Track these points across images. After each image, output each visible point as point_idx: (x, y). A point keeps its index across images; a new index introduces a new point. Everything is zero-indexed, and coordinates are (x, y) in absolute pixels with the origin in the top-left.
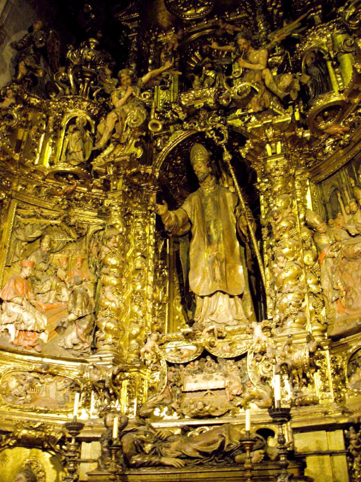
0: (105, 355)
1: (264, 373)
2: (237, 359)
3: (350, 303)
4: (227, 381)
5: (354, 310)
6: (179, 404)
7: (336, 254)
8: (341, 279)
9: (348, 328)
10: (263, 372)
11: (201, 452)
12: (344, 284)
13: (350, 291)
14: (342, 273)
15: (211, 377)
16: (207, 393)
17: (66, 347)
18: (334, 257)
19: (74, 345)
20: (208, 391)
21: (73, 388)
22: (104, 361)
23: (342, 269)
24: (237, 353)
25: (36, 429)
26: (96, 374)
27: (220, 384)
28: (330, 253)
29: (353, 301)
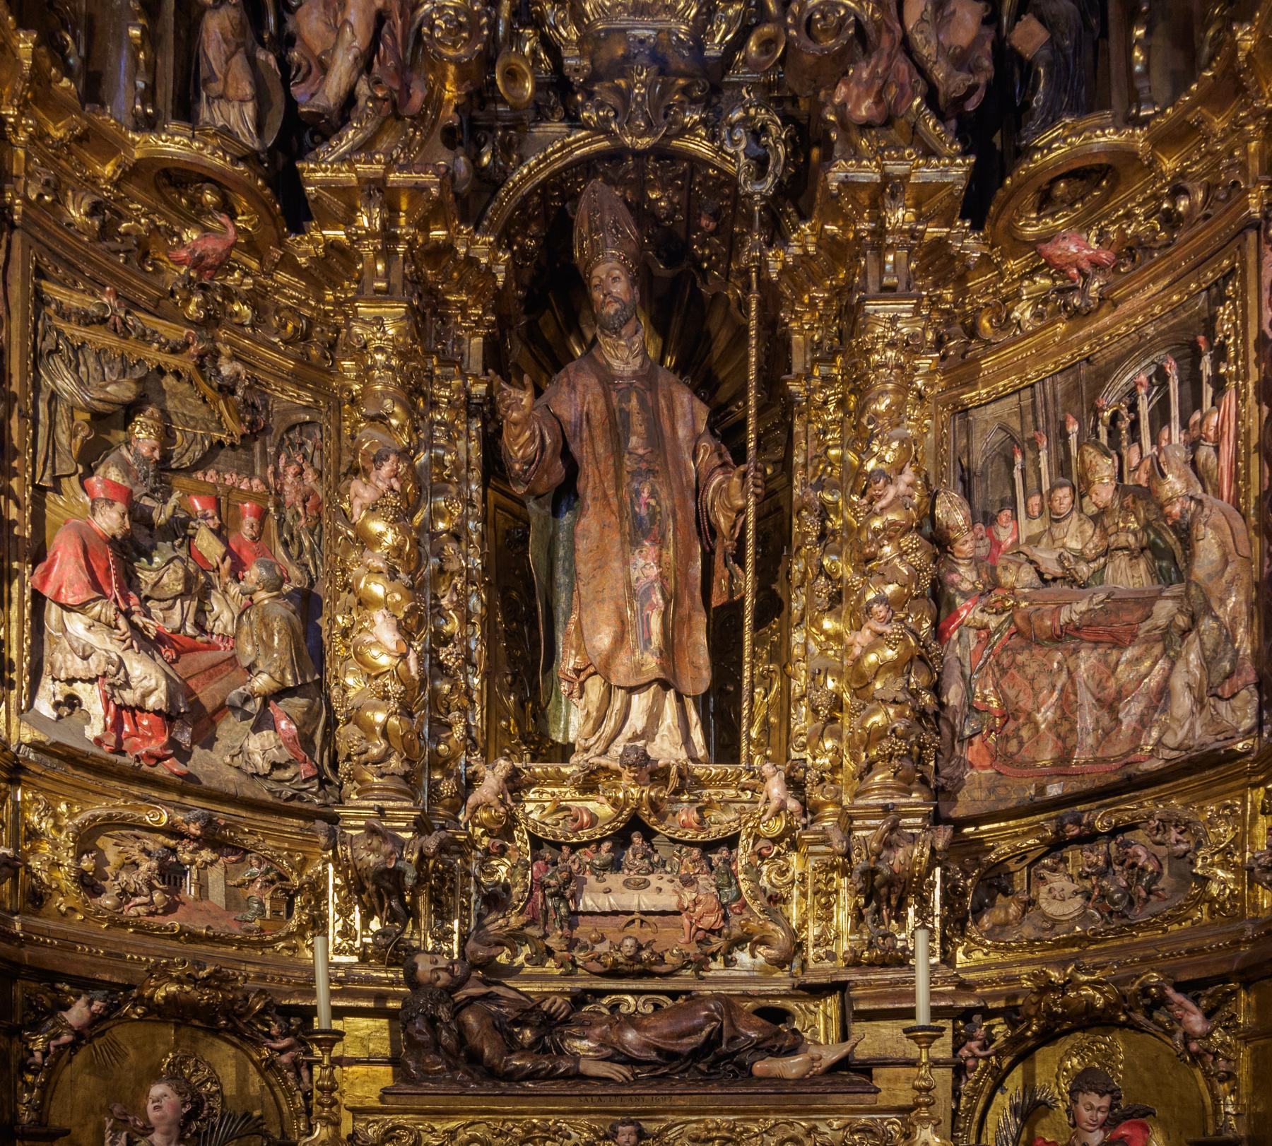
0: (391, 804)
1: (773, 886)
2: (708, 847)
3: (1013, 746)
4: (689, 895)
5: (1024, 765)
6: (572, 944)
7: (993, 622)
8: (997, 686)
9: (1002, 807)
10: (771, 882)
11: (659, 1051)
12: (1004, 701)
13: (1016, 719)
14: (1004, 671)
15: (646, 884)
16: (633, 921)
17: (250, 770)
18: (985, 627)
19: (275, 766)
20: (637, 916)
21: (272, 882)
22: (391, 820)
23: (1005, 661)
24: (714, 832)
25: (205, 983)
26: (373, 851)
27: (668, 901)
28: (978, 616)
29: (1021, 744)
